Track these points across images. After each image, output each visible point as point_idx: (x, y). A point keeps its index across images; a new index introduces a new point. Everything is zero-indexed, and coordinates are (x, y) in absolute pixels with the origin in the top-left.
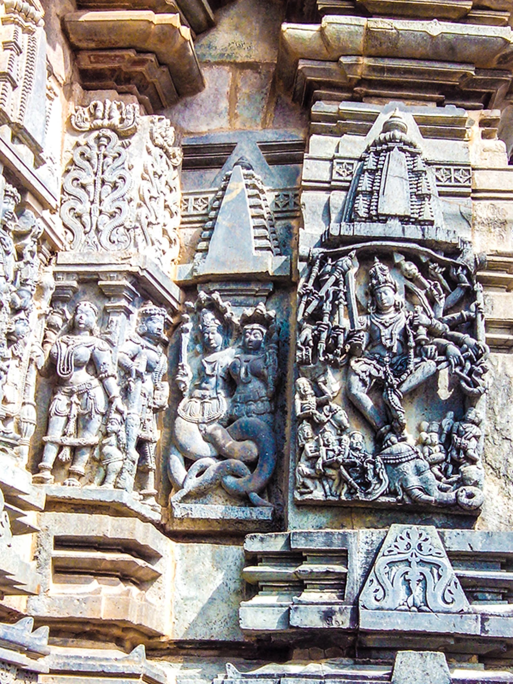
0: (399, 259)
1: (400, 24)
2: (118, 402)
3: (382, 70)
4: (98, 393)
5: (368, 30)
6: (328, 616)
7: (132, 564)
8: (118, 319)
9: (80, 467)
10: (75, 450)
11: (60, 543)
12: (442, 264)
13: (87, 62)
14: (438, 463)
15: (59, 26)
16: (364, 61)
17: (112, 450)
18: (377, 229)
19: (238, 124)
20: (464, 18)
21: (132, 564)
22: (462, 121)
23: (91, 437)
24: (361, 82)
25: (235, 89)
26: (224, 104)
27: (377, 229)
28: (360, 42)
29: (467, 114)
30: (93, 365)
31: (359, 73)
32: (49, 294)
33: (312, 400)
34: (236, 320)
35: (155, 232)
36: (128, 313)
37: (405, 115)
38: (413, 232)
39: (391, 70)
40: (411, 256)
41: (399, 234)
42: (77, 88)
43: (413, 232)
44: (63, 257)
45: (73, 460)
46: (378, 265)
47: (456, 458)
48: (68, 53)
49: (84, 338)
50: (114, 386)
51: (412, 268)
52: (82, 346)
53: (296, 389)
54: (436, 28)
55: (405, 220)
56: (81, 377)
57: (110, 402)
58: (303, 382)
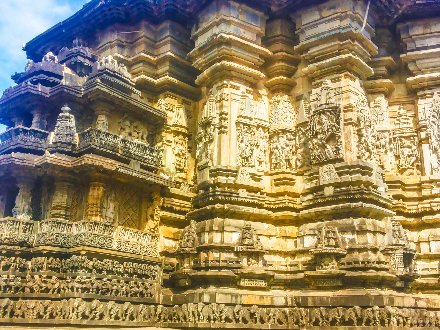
0: (326, 112)
1: (322, 62)
2: (281, 154)
3: (322, 72)
4: (278, 154)
5: (317, 66)
6: (316, 184)
7: (291, 182)
8: (281, 138)
9: (278, 167)
10: (276, 164)
11: (275, 180)
12: (333, 111)
13: (272, 89)
14: (335, 151)
15: (167, 154)
16: (318, 71)
17: (281, 163)
18: (321, 108)
19: (304, 89)
20: (338, 54)
21: (291, 182)
22: (340, 77)
23: (278, 161)
24: (320, 75)
25: (303, 82)
26: (301, 86)
27: (321, 108)
28: (316, 68)
29: (340, 75)
30: (277, 148)
31: (319, 74)
32: (268, 137)
33: (312, 145)
34: (304, 131)
35: (289, 119)
36: (283, 137)
37: (327, 81)
38: (327, 106)
39: (324, 71)
40: (328, 111)
41: (324, 108)
42: (271, 95)
43: (327, 106)
44: (270, 130)
45: (276, 166)
46: (322, 115)
47: (337, 150)
48: (267, 89)
49: (276, 143)
50: (281, 151)
51: (328, 114)
52: (274, 145)
53: (309, 144)
54: (328, 61)
55: (325, 104)
56: (276, 151)
57: (280, 154)
58: (310, 142)
